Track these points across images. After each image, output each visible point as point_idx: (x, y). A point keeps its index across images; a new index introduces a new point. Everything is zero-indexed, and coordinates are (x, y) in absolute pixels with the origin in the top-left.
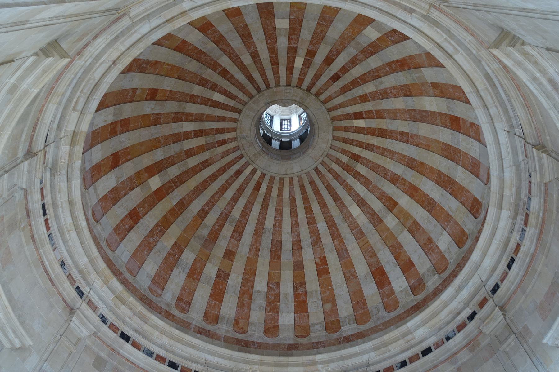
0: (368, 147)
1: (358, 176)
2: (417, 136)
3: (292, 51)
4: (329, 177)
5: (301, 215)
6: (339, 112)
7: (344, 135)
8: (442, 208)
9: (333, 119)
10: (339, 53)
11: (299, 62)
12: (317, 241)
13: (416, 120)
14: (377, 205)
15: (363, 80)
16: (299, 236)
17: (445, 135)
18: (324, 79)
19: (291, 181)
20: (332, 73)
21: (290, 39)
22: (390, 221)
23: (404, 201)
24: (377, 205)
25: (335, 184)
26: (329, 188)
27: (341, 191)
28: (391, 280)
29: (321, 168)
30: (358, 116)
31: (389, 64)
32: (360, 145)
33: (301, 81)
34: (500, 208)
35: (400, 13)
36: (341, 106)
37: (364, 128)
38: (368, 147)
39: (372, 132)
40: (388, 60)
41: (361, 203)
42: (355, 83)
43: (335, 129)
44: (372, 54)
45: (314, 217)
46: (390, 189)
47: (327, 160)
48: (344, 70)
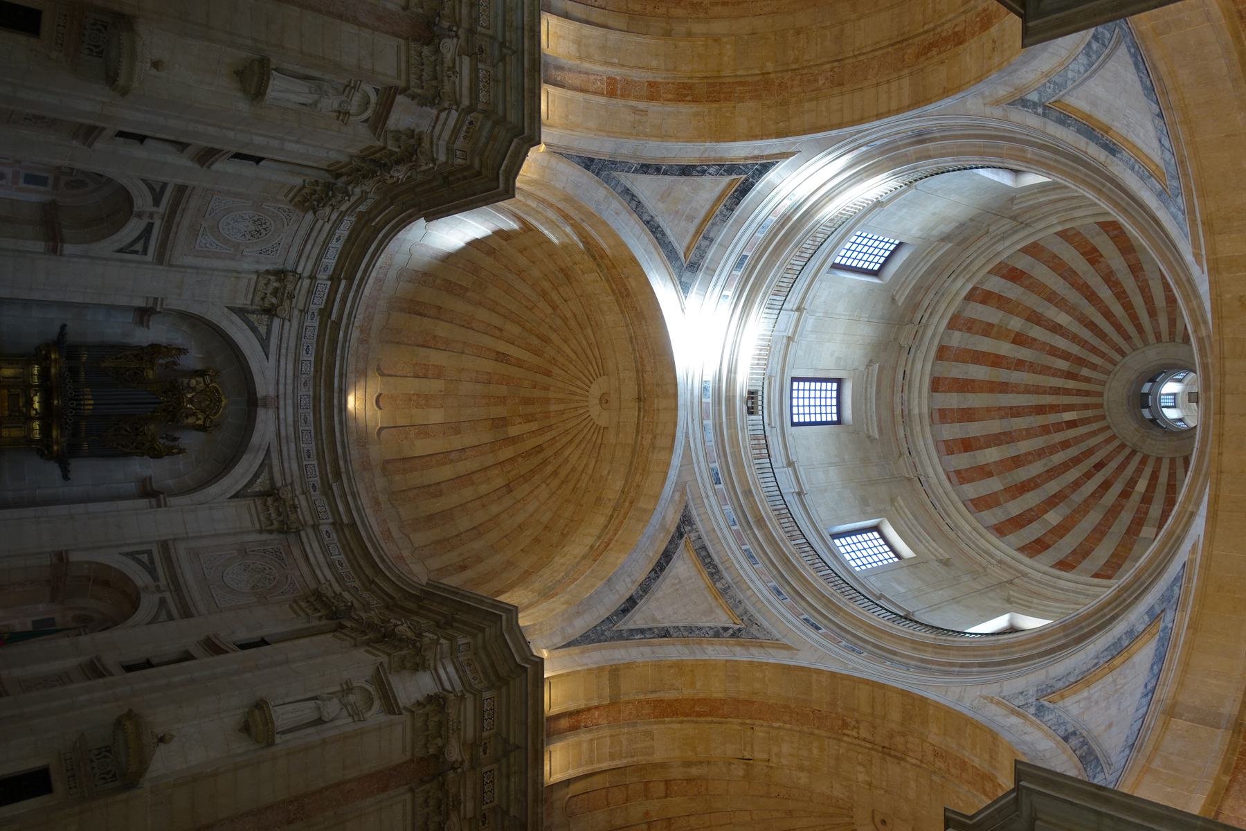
0: (1056, 391)
1: (1066, 356)
2: (1002, 418)
3: (1147, 499)
4: (1104, 348)
5: (1138, 301)
6: (1095, 426)
7: (1087, 400)
8: (964, 362)
9: (1103, 417)
10: (1093, 495)
11: (1141, 486)
12: (1109, 278)
13: (1005, 433)
14: (1037, 332)
15: (1066, 466)
16: (1136, 278)
17: (974, 429)
18: (1113, 465)
19: (1158, 338)
20: (1102, 472)
21: (1146, 513)
22: (1016, 324)
23: (1005, 348)
24: (1037, 332)
25: (1095, 341)
26: (1102, 335)
27: (1086, 334)
28: (1003, 281)
29: (1117, 357)
30: (1072, 424)
31: (1037, 486)
32: (1067, 392)
33: (1143, 462)
34: (920, 415)
35: (1008, 560)
36: (1094, 434)
37: (1064, 411)
38: (1056, 391)
39: (1054, 409)
40: (1038, 490)
41: (1056, 329)
42: (1076, 461)
43: (1100, 406)
44: (1054, 496)
45: (1118, 299)
46: (1025, 354)
47: (1110, 367)
48: (1088, 476)
